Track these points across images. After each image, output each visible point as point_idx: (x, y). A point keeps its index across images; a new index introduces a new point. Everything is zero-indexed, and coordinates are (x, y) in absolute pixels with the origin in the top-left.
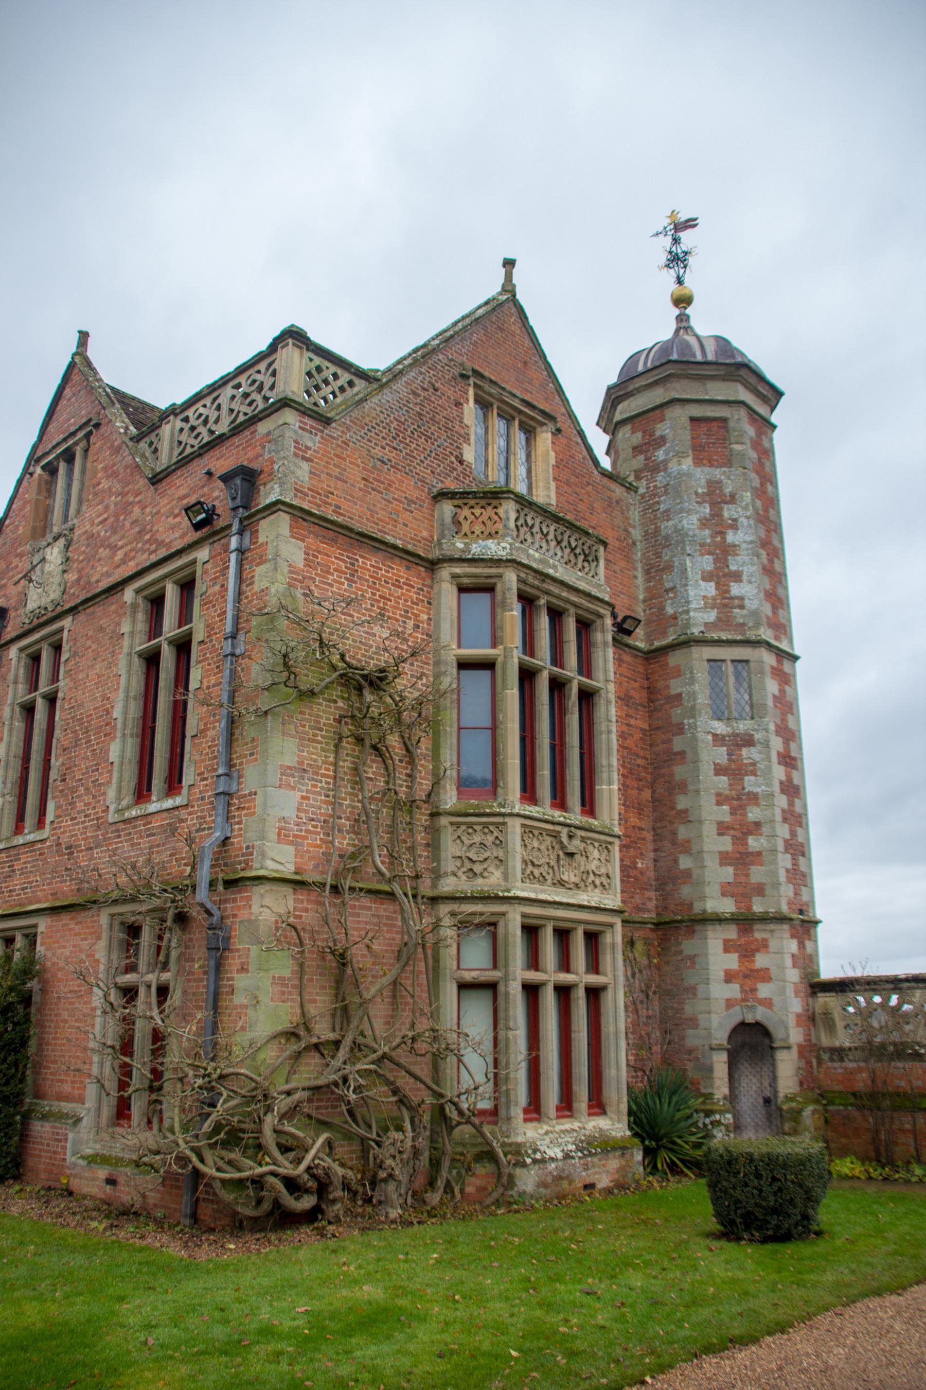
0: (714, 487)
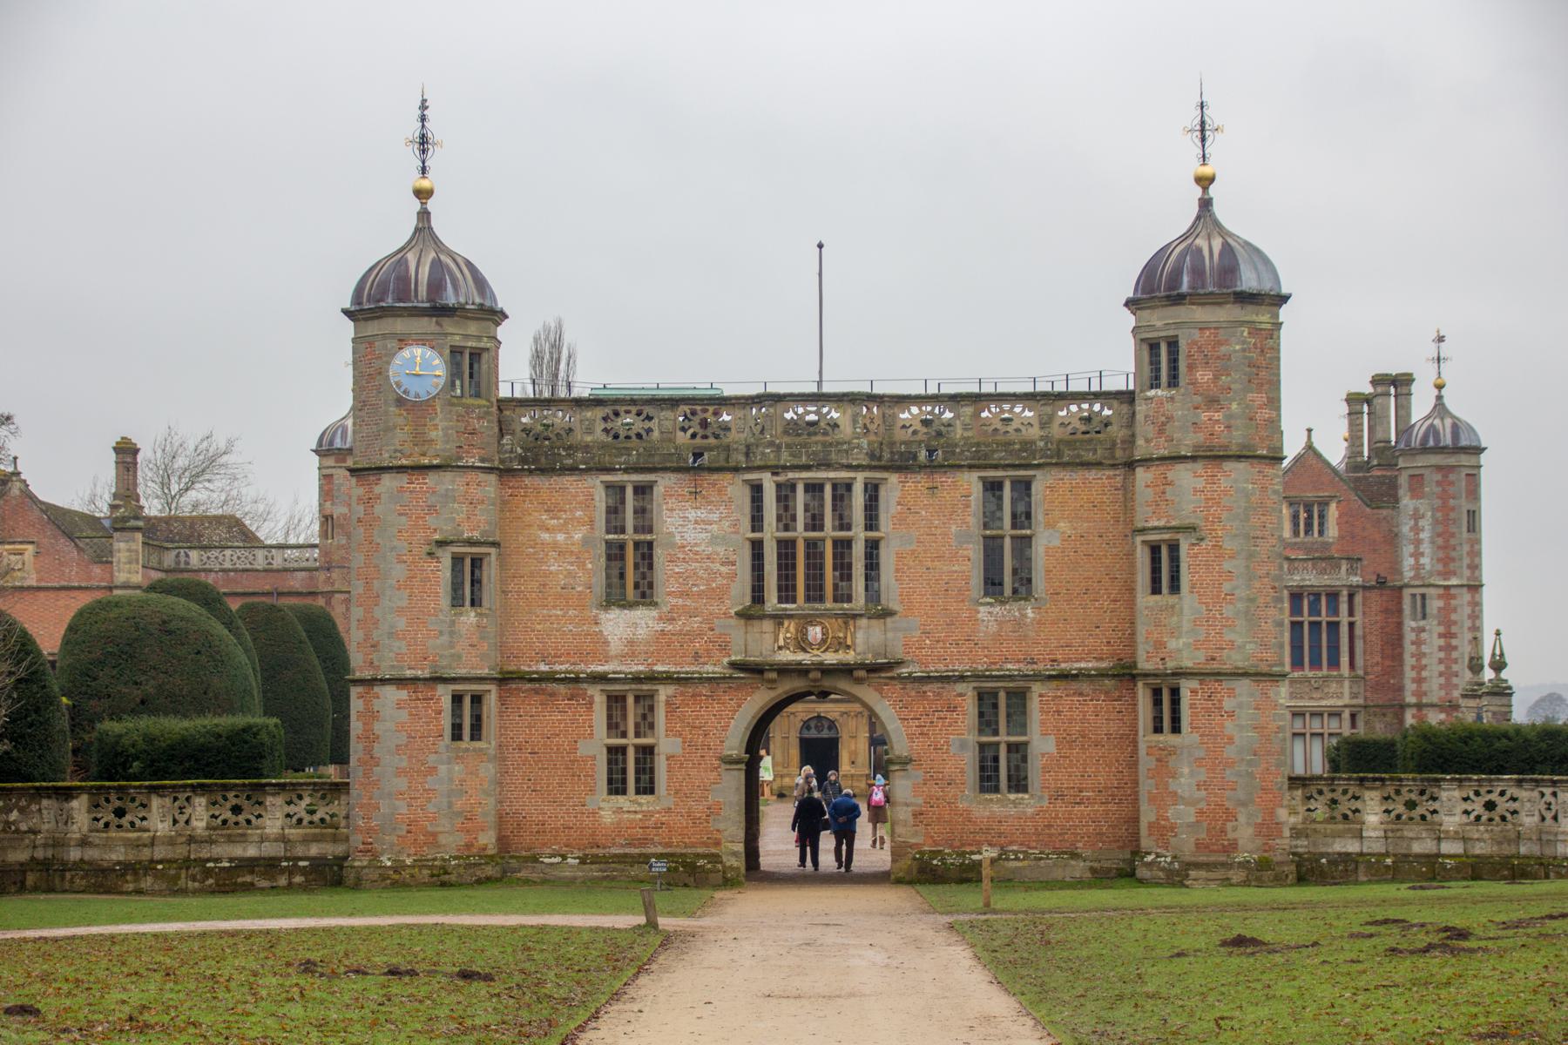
0: (1416, 510)
